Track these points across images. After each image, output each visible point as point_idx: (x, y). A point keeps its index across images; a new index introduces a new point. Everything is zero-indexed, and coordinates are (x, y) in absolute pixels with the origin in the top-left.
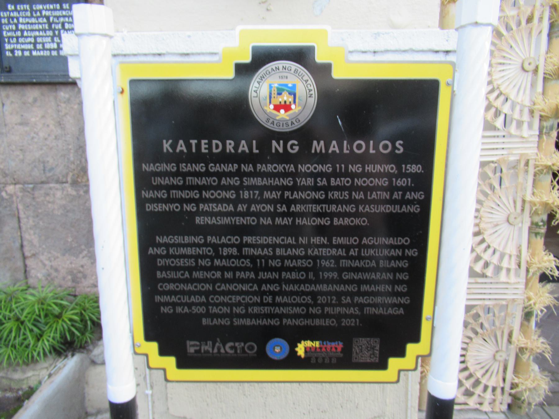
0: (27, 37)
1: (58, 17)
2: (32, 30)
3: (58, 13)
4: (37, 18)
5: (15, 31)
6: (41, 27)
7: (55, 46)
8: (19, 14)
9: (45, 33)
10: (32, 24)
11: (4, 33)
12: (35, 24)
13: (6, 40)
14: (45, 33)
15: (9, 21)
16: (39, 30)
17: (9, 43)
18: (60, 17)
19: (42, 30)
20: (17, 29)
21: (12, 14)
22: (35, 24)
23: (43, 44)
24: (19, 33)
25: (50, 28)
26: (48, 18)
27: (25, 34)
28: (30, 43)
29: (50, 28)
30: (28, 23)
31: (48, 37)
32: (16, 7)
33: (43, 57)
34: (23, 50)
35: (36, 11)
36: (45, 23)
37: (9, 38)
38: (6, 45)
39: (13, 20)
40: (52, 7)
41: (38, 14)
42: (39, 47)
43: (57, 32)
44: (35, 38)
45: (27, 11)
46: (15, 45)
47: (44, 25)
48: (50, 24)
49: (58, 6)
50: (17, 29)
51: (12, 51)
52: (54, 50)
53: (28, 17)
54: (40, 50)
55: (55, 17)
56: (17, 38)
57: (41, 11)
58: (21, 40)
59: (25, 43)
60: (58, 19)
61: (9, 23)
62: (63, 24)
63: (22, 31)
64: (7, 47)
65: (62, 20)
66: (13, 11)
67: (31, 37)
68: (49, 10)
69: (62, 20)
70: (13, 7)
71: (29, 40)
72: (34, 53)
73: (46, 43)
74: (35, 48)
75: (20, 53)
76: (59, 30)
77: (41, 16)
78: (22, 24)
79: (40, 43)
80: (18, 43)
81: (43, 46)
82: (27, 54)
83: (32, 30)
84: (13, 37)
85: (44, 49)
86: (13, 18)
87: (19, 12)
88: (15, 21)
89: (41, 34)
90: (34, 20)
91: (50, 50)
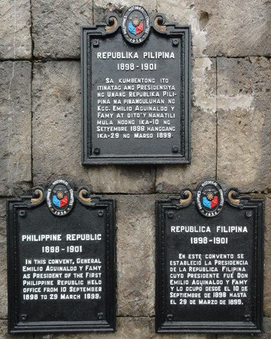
0: (194, 286)
1: (230, 267)
2: (201, 279)
3: (233, 263)
4: (208, 267)
5: (183, 280)
6: (211, 276)
7: (225, 295)
8: (189, 263)
9: (215, 282)
10: (202, 273)
11: (171, 281)
12: (205, 273)
13: (172, 288)
14: (215, 282)
15: (177, 270)
16: (209, 279)
17: (175, 291)
18: (233, 266)
19: (212, 279)
20: (186, 278)
21: (181, 263)
22: (205, 273)
23: (212, 293)
24: (187, 282)
25: (221, 278)
26: (220, 267)
27: (194, 282)
28: (198, 292)
29: (221, 278)
30: (198, 272)
31: (217, 286)
32: (187, 256)
33: (211, 305)
34: (188, 299)
35: (208, 261)
36: (216, 272)
37: (175, 286)
38: (171, 293)
39: (182, 269)
40: (225, 256)
41: (210, 263)
42: (207, 295)
43: (228, 282)
44: (204, 286)
45: (200, 260)
46: (181, 294)
47: (214, 274)
48: (221, 273)
49: (232, 256)
50: (186, 278)
51: (177, 300)
52: (223, 298)
53: (198, 266)
54: (207, 299)
55: (227, 266)
56: (184, 286)
57: (213, 260)
58: (187, 289)
59: (193, 292)
60: (230, 269)
61: (178, 272)
62: (235, 273)
63: (191, 280)
64: (172, 295)
65: (234, 269)
66: (183, 260)
67: (199, 286)
68: (221, 260)
69: (234, 269)
70: (184, 256)
71: (197, 288)
72: (201, 302)
73: (215, 292)
74: (202, 298)
75: (185, 302)
76: (231, 279)
77: (213, 265)
78: (191, 273)
79: (208, 292)
80: (184, 291)
81: (212, 295)
82: (193, 302)
83: (201, 279)
84: (179, 286)
85: (212, 298)
86: (182, 267)
87: (189, 260)
88: (185, 270)
89: (211, 283)
90: (204, 269)
91: (218, 299)
